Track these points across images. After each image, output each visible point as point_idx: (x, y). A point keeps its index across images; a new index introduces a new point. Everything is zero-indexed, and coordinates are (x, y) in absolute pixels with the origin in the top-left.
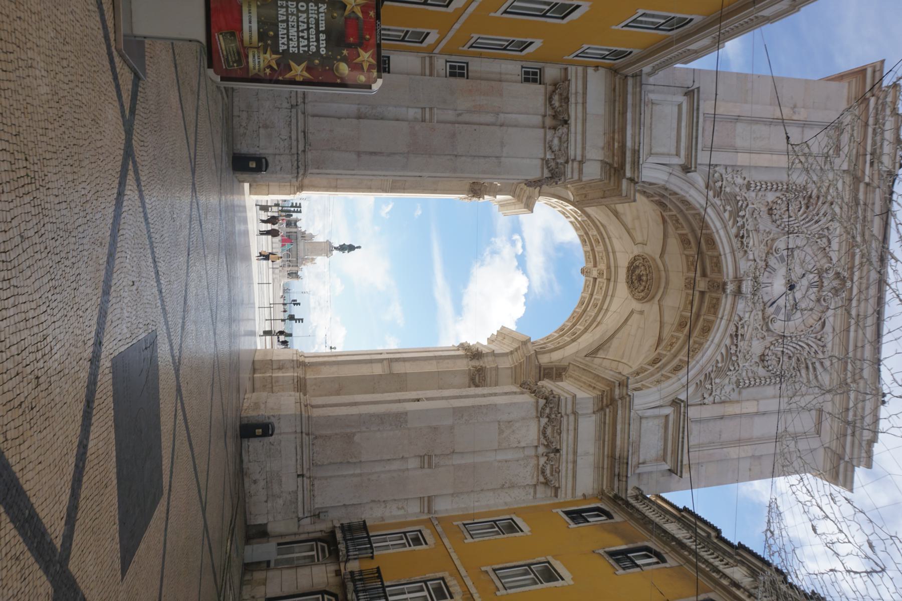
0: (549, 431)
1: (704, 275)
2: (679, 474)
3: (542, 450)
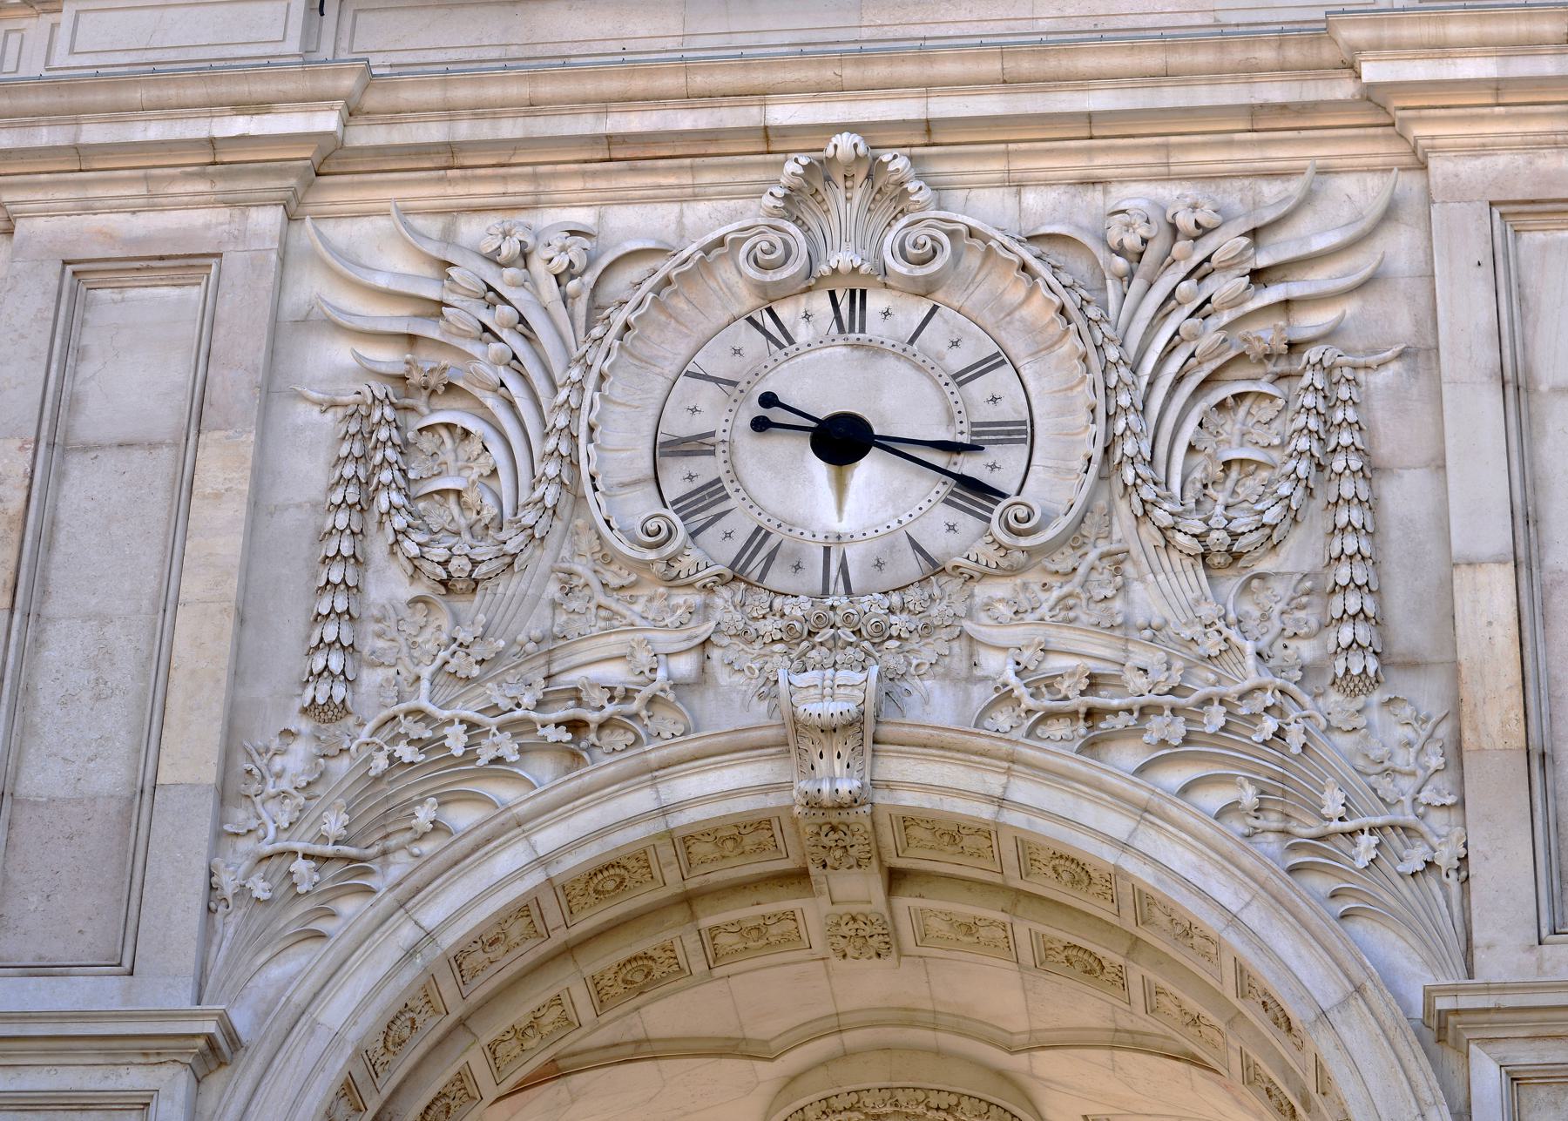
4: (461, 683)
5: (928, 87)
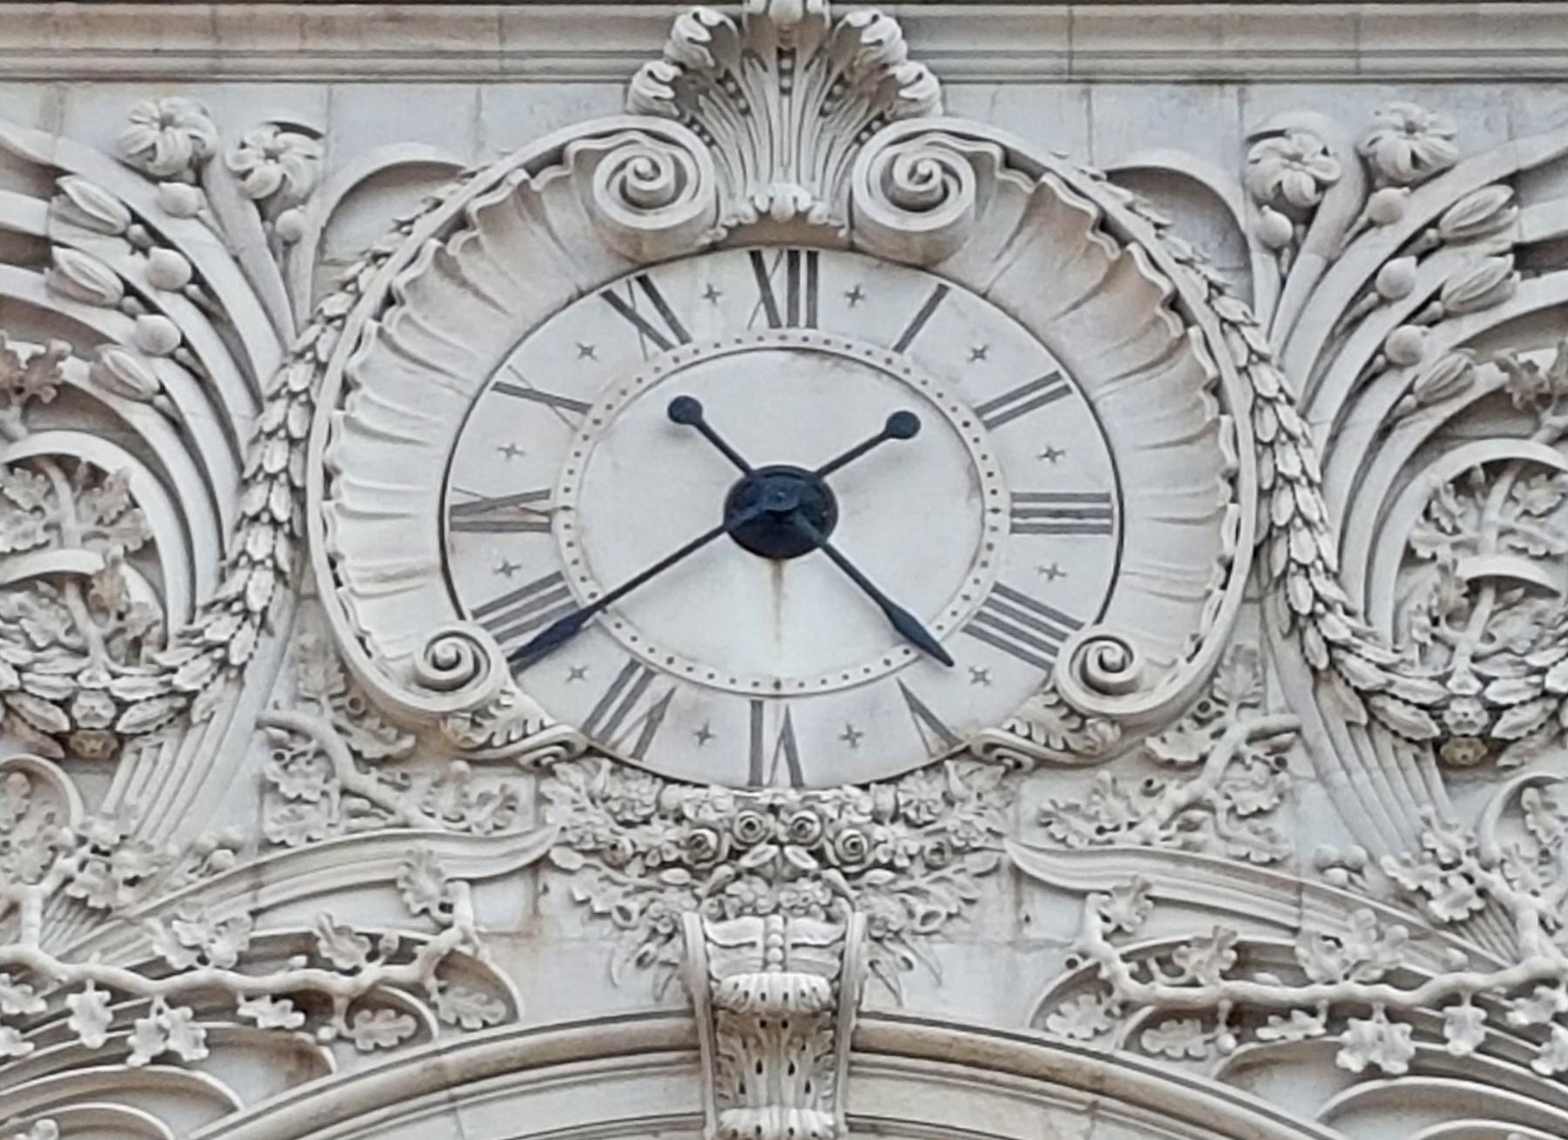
4: (94, 919)
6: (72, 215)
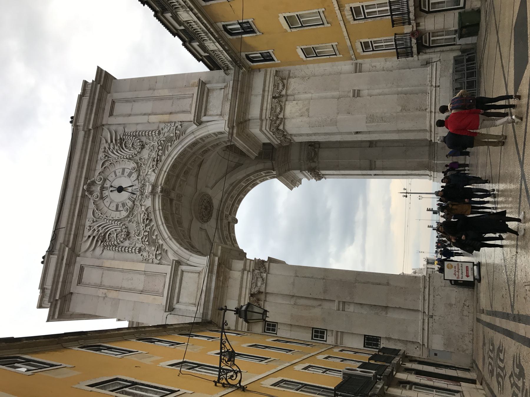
0: (278, 110)
1: (171, 200)
2: (201, 81)
3: (284, 99)
5: (81, 177)
6: (92, 235)
